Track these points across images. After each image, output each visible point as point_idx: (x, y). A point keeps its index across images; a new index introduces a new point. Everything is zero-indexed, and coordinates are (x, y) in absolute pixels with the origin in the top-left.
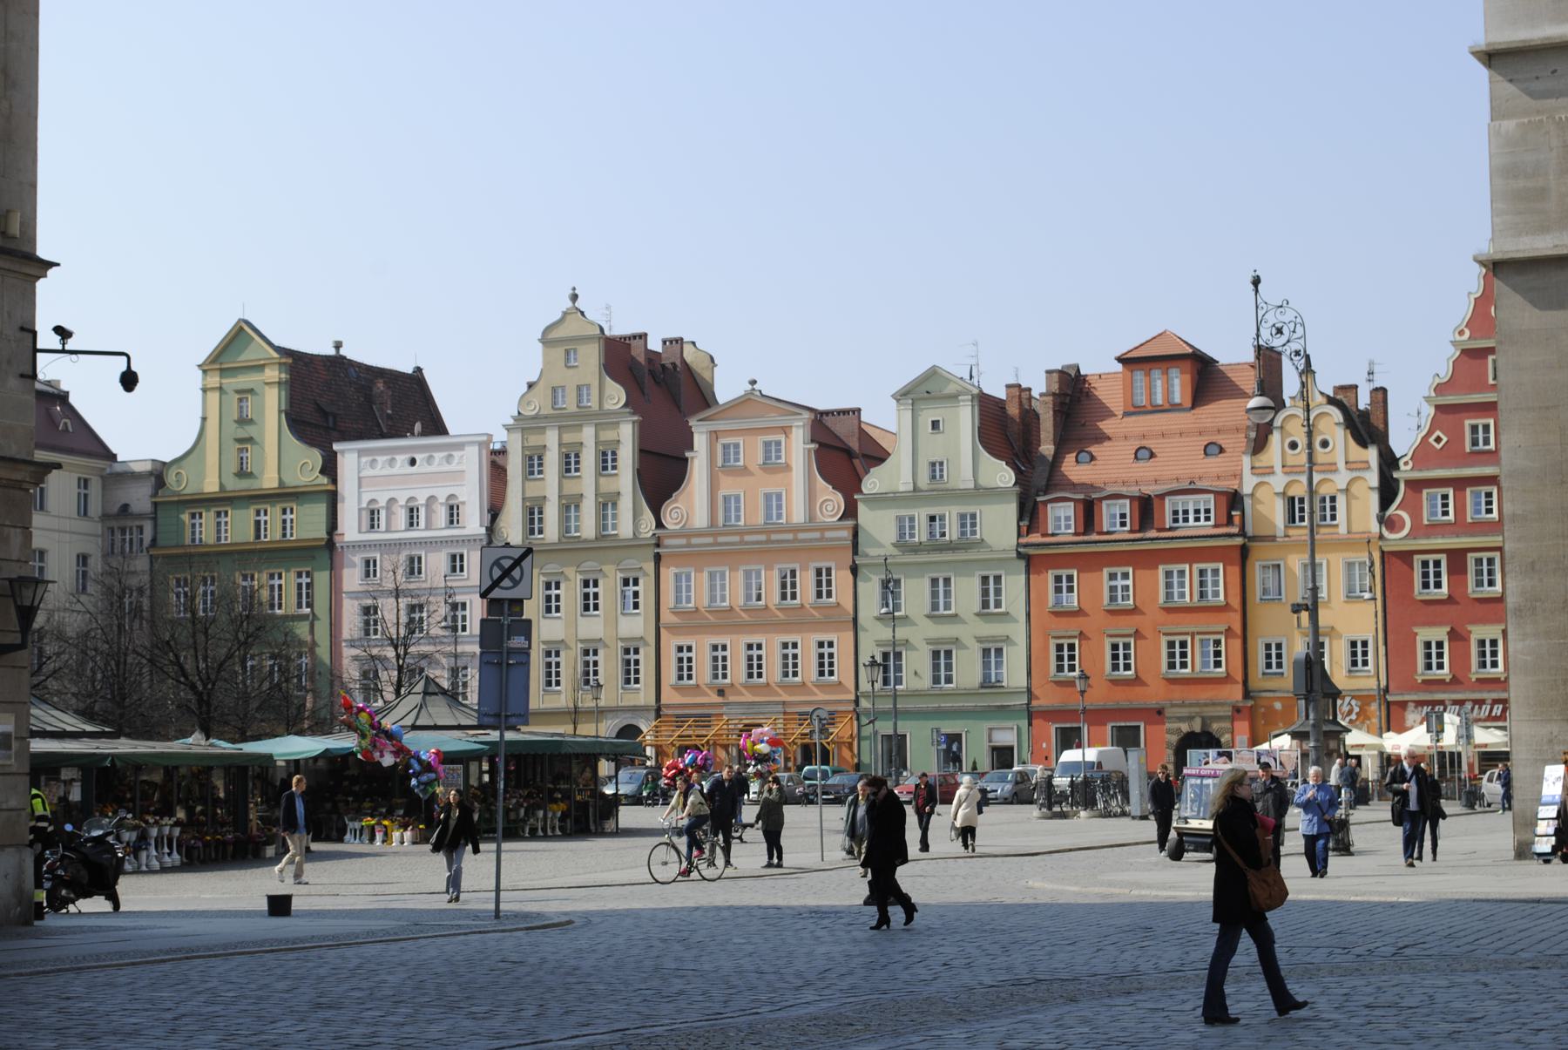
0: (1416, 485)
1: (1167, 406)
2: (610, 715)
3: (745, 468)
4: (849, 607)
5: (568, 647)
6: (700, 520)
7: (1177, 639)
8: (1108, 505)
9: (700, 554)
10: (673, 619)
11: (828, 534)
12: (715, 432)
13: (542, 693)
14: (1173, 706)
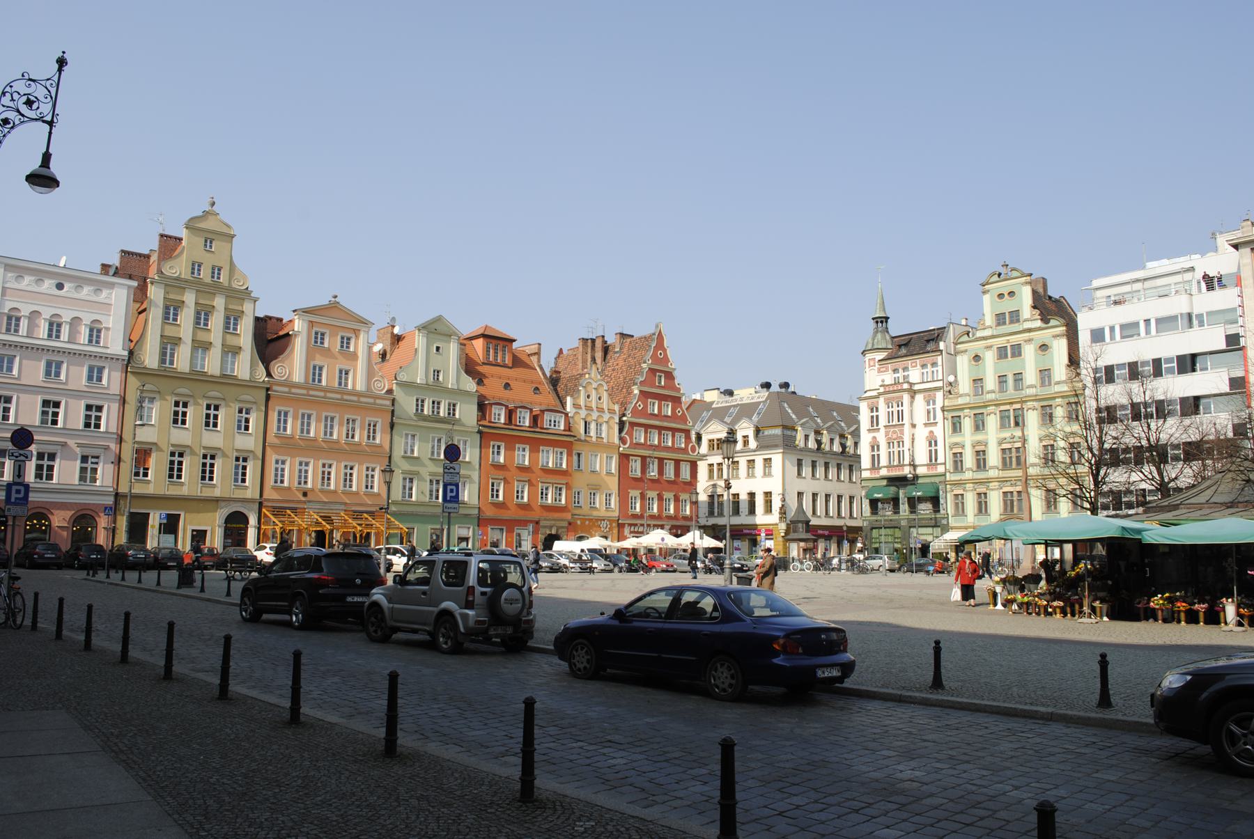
0: (633, 425)
1: (501, 364)
2: (223, 504)
3: (329, 349)
4: (387, 447)
5: (159, 449)
6: (298, 376)
7: (559, 486)
8: (520, 412)
9: (297, 400)
10: (276, 441)
11: (378, 401)
12: (312, 322)
13: (200, 485)
14: (545, 520)
